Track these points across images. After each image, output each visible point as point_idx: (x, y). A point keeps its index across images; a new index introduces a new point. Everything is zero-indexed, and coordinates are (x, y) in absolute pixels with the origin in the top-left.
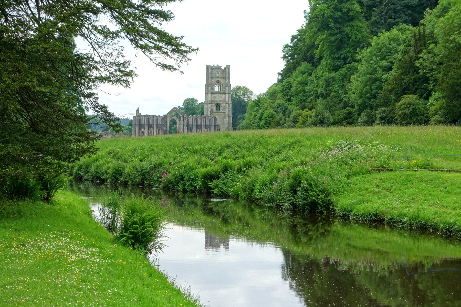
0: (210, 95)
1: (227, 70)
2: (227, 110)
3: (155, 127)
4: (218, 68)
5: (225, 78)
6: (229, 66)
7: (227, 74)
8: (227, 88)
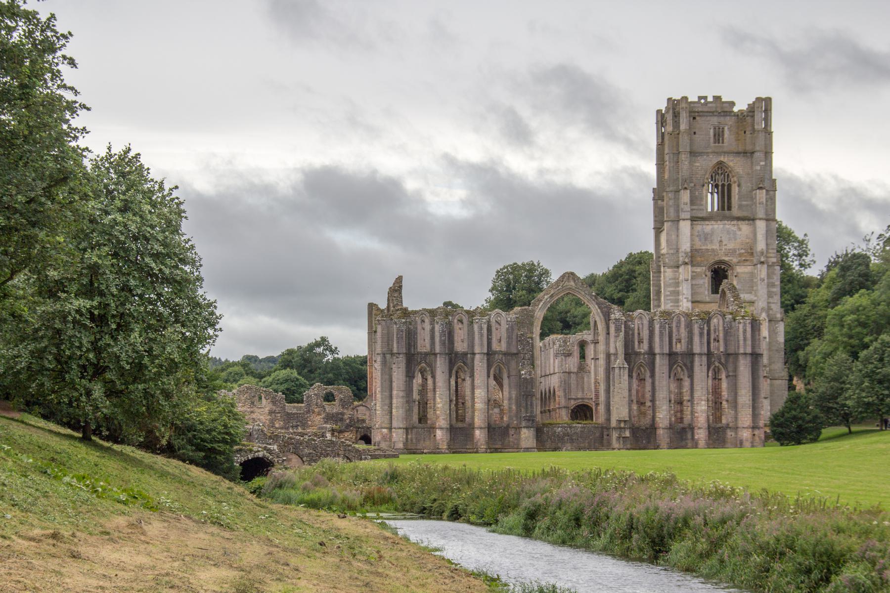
0: (685, 227)
1: (760, 116)
2: (762, 290)
3: (480, 364)
4: (720, 108)
5: (748, 154)
6: (768, 101)
7: (762, 136)
8: (761, 195)
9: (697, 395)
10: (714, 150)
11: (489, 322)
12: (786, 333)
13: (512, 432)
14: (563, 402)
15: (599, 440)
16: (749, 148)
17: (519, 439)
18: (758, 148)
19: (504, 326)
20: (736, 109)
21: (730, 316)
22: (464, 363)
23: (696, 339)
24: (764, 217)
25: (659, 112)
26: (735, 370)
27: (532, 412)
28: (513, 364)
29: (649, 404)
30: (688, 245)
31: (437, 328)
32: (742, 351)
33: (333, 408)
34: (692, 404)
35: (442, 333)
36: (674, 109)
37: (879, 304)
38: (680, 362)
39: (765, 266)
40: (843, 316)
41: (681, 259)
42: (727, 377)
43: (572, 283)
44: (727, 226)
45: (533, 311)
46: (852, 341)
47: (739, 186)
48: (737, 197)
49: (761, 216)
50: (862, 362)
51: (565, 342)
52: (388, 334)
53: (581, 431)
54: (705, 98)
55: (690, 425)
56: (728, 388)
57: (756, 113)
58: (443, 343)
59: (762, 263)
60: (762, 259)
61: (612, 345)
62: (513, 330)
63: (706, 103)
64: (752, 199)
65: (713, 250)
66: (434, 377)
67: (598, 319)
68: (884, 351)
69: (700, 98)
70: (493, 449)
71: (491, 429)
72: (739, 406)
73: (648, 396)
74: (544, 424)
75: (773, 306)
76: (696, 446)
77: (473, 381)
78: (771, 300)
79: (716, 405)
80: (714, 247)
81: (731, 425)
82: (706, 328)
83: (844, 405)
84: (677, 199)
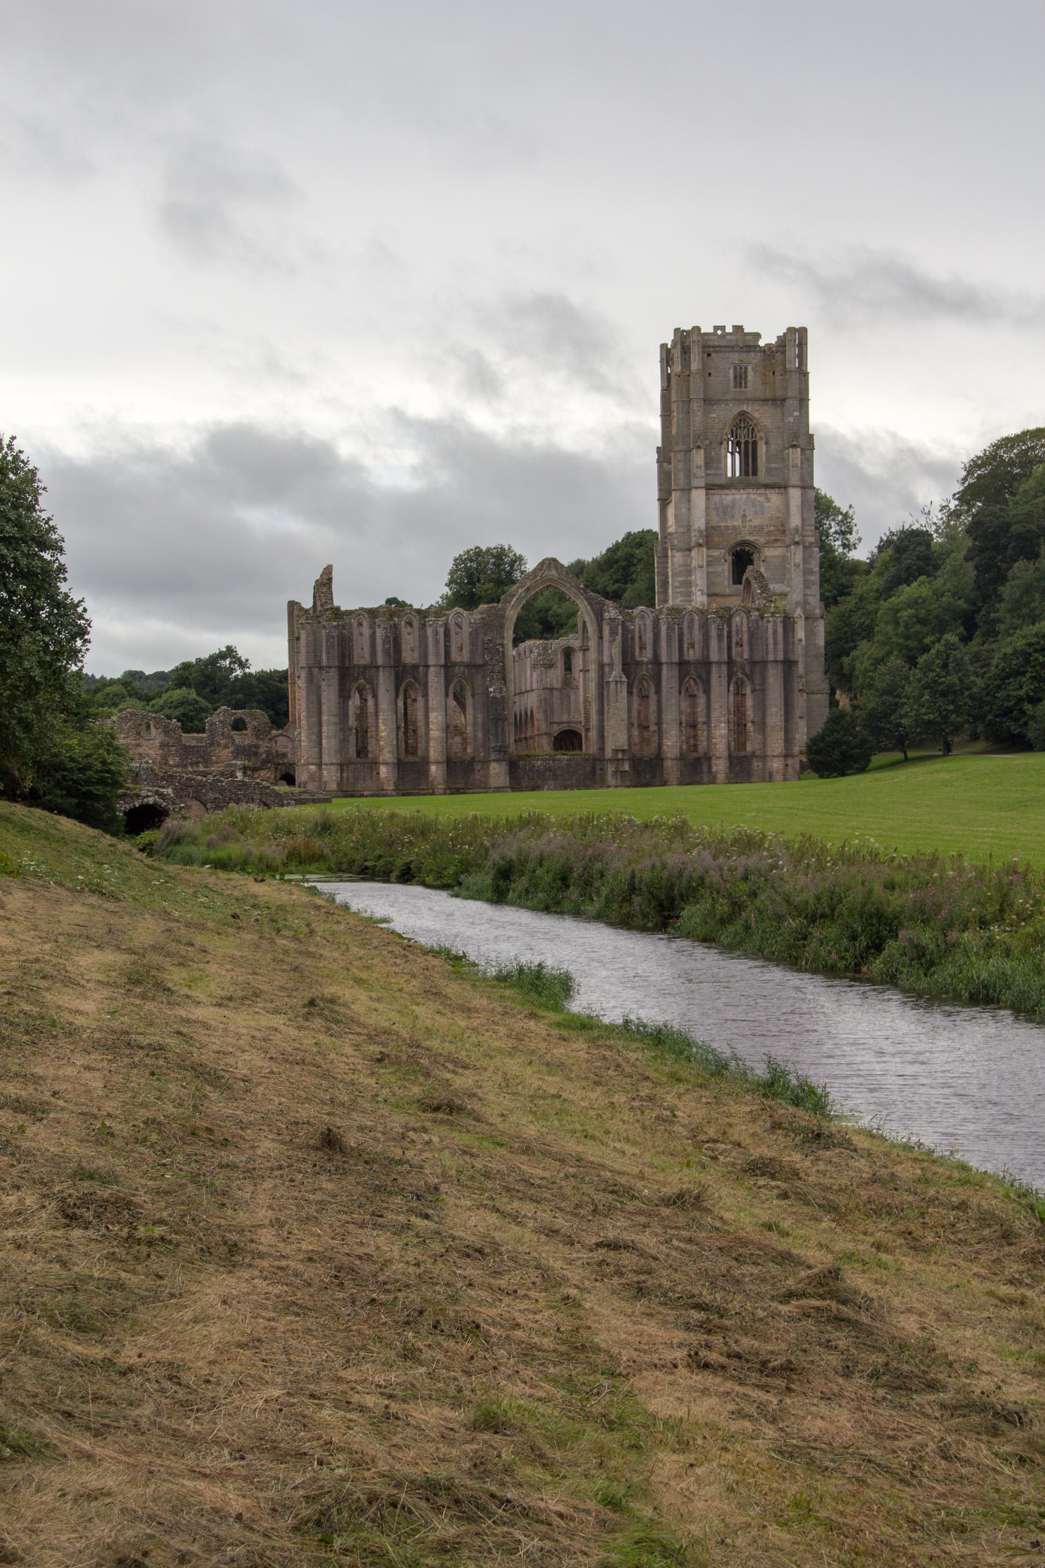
0: (699, 497)
1: (792, 351)
3: (435, 680)
4: (742, 341)
5: (778, 401)
6: (803, 332)
7: (795, 377)
8: (795, 456)
9: (715, 715)
10: (735, 396)
11: (446, 625)
12: (828, 633)
13: (478, 767)
14: (543, 728)
15: (591, 776)
16: (779, 394)
17: (487, 776)
18: (790, 394)
19: (466, 630)
20: (762, 343)
21: (757, 613)
22: (414, 678)
23: (714, 643)
24: (799, 483)
25: (663, 346)
26: (764, 681)
27: (503, 741)
28: (479, 679)
29: (653, 728)
31: (379, 633)
32: (771, 658)
33: (245, 738)
34: (709, 726)
35: (386, 641)
36: (683, 343)
37: (942, 595)
38: (694, 673)
39: (801, 547)
40: (898, 611)
41: (694, 539)
42: (753, 691)
43: (554, 572)
44: (752, 497)
45: (504, 609)
46: (909, 642)
47: (767, 443)
48: (764, 457)
49: (795, 483)
50: (921, 669)
51: (545, 649)
52: (315, 641)
53: (567, 765)
54: (723, 328)
55: (705, 754)
56: (754, 707)
57: (787, 348)
58: (386, 652)
59: (797, 543)
60: (797, 539)
61: (606, 653)
62: (477, 634)
63: (725, 335)
64: (784, 460)
65: (734, 528)
66: (375, 697)
67: (587, 619)
68: (948, 655)
69: (716, 328)
70: (454, 790)
71: (451, 764)
72: (769, 729)
73: (653, 717)
74: (519, 757)
75: (810, 599)
76: (713, 781)
77: (427, 701)
78: (808, 592)
79: (739, 728)
80: (736, 524)
81: (758, 753)
82: (726, 629)
83: (899, 725)
84: (688, 461)
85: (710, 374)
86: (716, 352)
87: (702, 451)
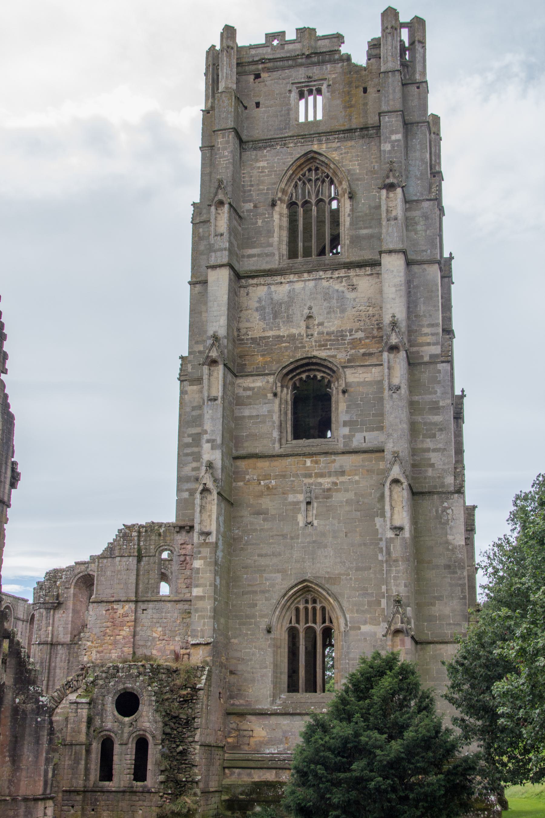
6: (417, 25)
24: (400, 246)
30: (223, 321)
39: (402, 354)
44: (325, 283)
48: (348, 220)
49: (391, 247)
59: (393, 349)
60: (394, 340)
63: (284, 43)
65: (292, 338)
69: (270, 37)
80: (294, 331)
85: (258, 105)
86: (268, 70)
87: (226, 206)
